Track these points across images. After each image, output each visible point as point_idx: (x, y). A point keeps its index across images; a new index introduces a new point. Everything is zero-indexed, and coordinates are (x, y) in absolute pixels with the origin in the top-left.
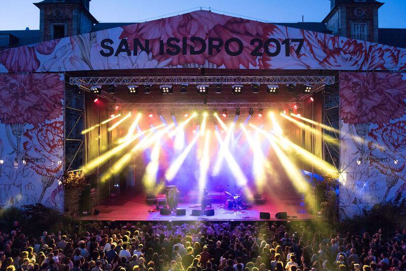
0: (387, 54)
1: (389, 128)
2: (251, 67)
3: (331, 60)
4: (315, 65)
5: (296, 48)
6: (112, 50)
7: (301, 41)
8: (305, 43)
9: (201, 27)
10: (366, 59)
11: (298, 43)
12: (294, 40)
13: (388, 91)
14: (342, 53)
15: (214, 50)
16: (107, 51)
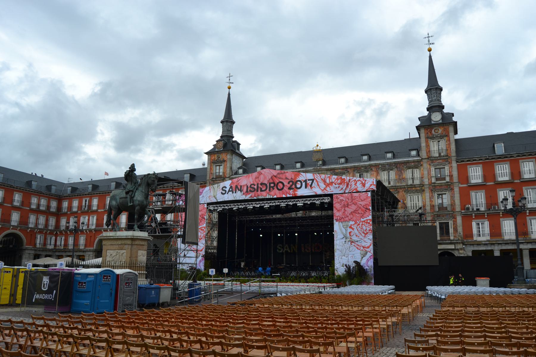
0: (359, 182)
1: (361, 223)
2: (288, 196)
3: (328, 189)
4: (319, 192)
5: (310, 184)
6: (226, 191)
7: (313, 180)
8: (315, 181)
9: (265, 178)
10: (347, 186)
11: (311, 181)
12: (309, 180)
13: (360, 203)
14: (334, 184)
15: (271, 188)
16: (224, 192)
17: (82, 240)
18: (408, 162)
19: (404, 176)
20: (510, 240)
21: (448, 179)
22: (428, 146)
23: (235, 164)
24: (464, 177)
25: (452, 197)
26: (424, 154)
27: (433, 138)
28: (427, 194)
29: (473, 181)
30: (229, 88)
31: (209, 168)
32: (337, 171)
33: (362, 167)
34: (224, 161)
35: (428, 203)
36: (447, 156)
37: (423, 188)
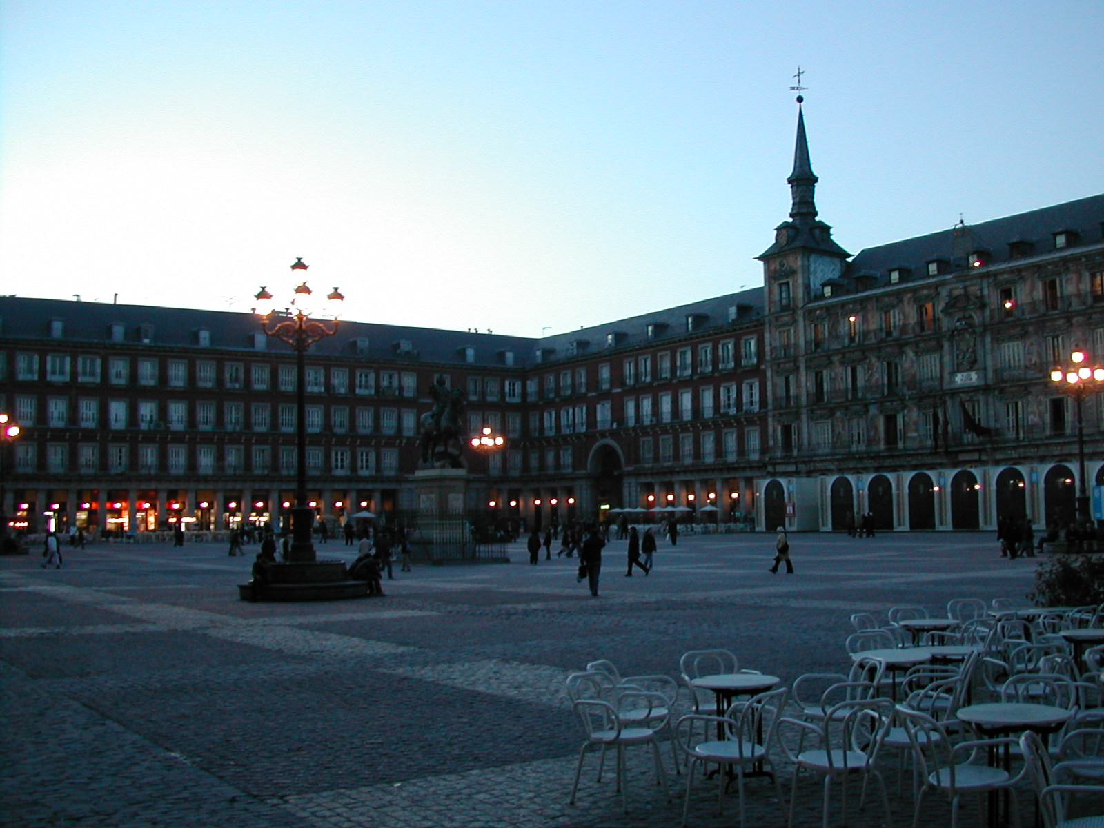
17: (567, 458)
23: (819, 275)
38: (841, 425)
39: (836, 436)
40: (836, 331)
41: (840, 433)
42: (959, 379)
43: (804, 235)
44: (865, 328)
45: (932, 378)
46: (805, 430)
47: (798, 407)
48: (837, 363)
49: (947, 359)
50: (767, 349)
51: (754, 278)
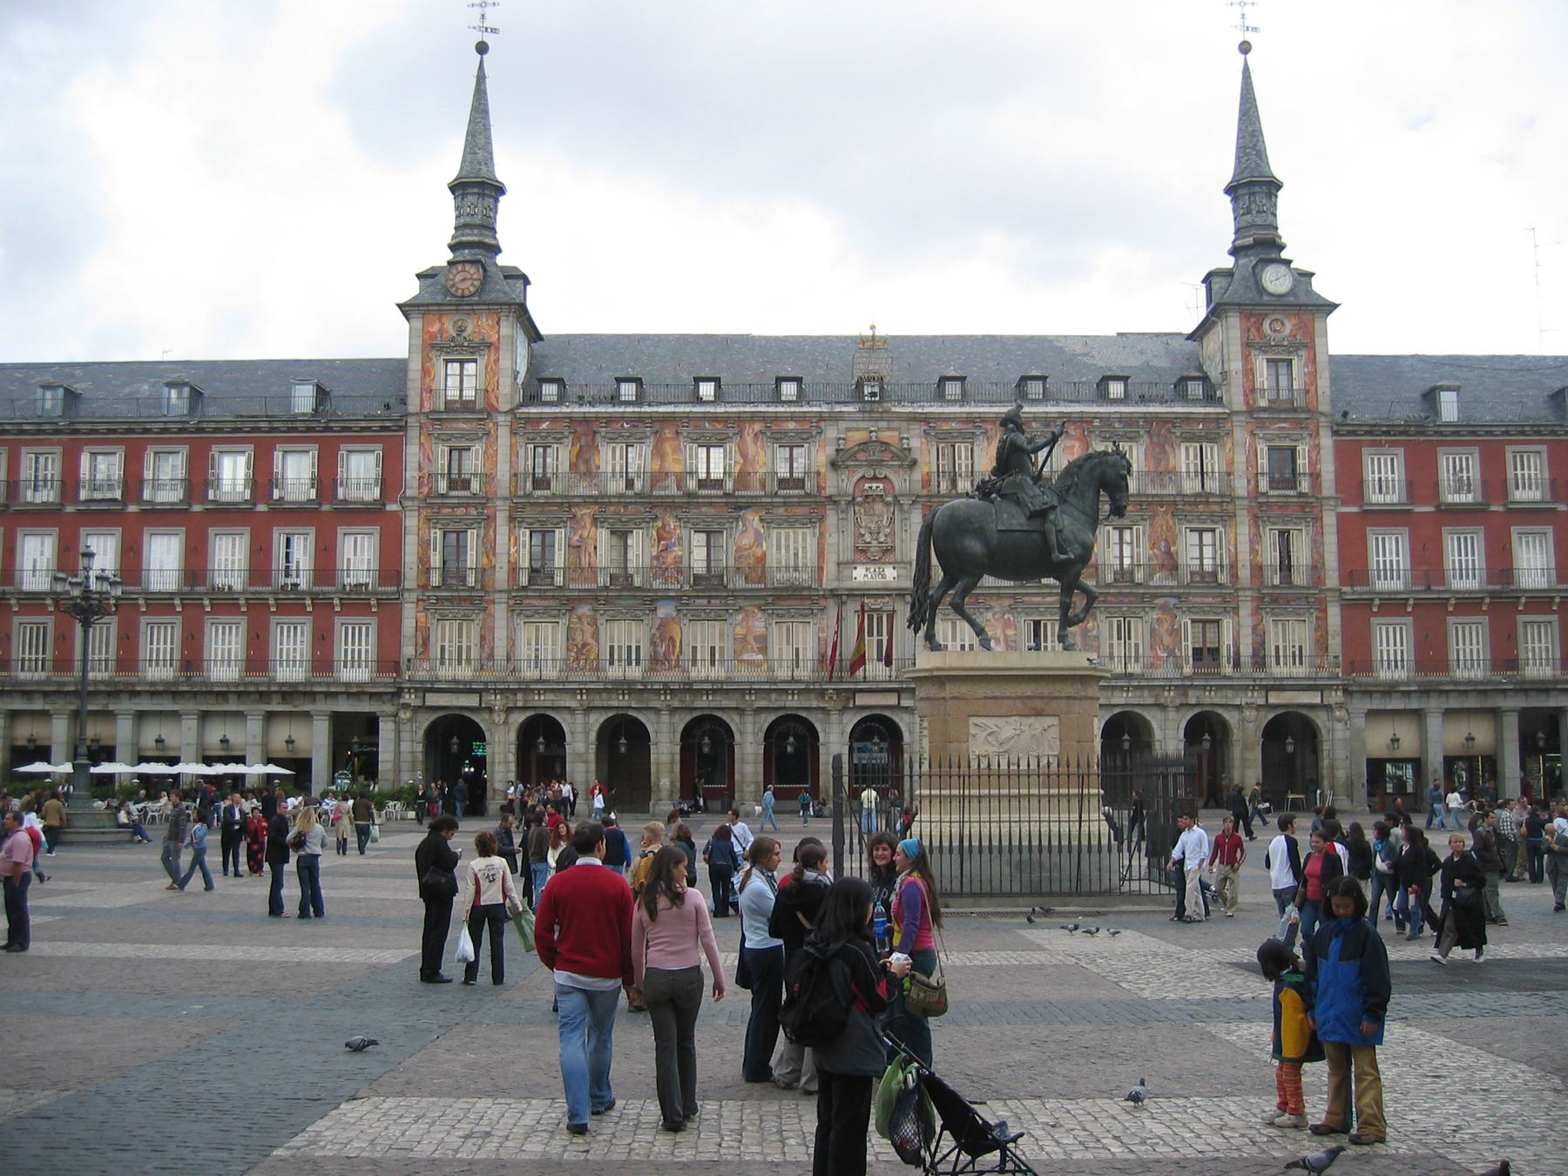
18: (1187, 419)
19: (1171, 464)
20: (1470, 682)
21: (1305, 485)
22: (1249, 372)
24: (1351, 482)
25: (1317, 544)
26: (1236, 400)
27: (1264, 347)
28: (1244, 529)
29: (1376, 498)
30: (482, 48)
31: (415, 367)
32: (945, 427)
33: (1035, 419)
34: (489, 346)
35: (1244, 557)
36: (1309, 411)
37: (1230, 508)
38: (589, 630)
39: (578, 651)
40: (587, 462)
41: (585, 645)
42: (861, 575)
43: (471, 289)
44: (656, 467)
45: (796, 569)
46: (500, 633)
47: (484, 584)
48: (588, 521)
49: (831, 539)
50: (411, 474)
51: (391, 339)
